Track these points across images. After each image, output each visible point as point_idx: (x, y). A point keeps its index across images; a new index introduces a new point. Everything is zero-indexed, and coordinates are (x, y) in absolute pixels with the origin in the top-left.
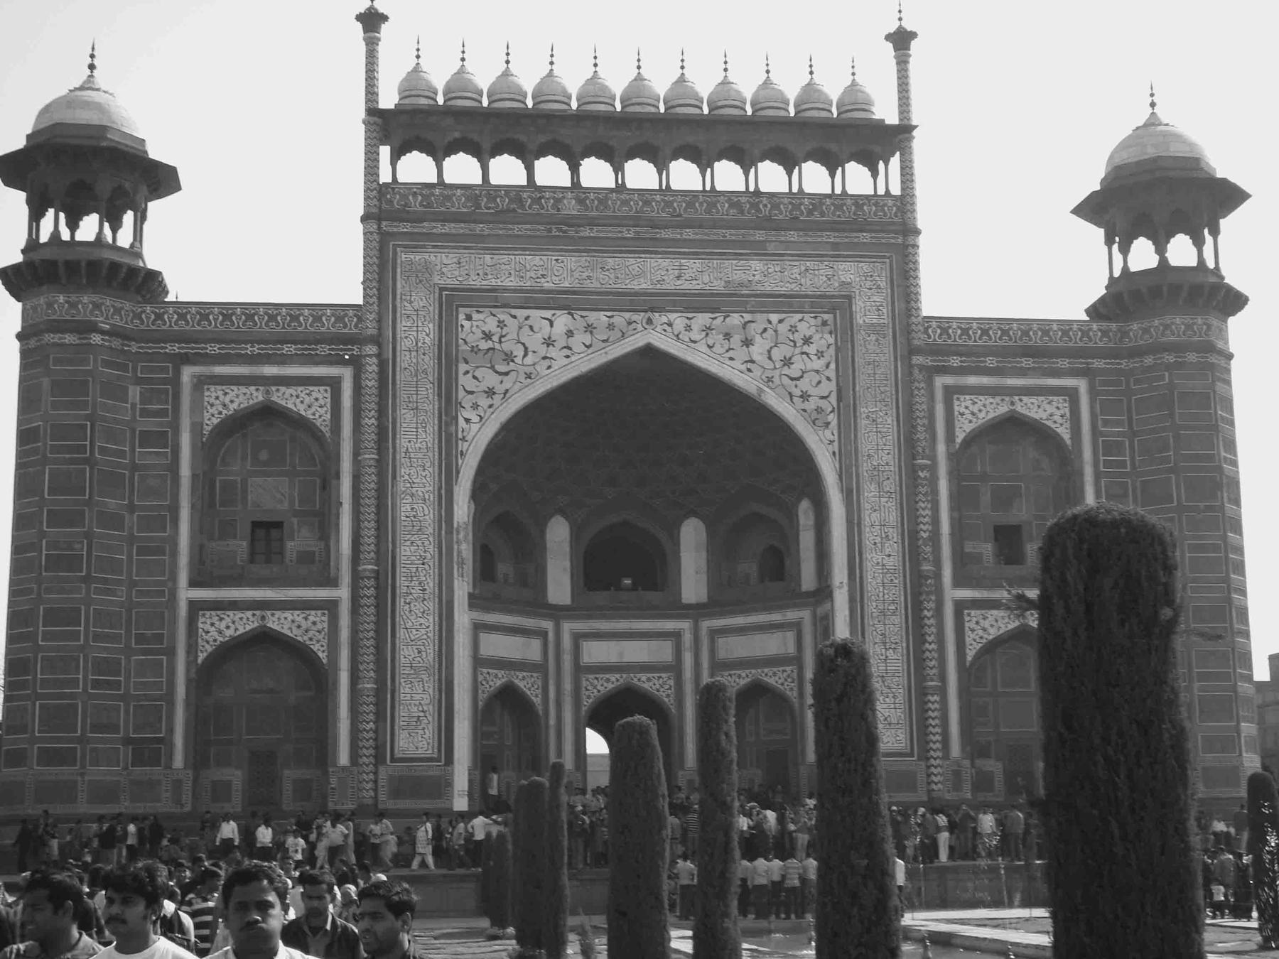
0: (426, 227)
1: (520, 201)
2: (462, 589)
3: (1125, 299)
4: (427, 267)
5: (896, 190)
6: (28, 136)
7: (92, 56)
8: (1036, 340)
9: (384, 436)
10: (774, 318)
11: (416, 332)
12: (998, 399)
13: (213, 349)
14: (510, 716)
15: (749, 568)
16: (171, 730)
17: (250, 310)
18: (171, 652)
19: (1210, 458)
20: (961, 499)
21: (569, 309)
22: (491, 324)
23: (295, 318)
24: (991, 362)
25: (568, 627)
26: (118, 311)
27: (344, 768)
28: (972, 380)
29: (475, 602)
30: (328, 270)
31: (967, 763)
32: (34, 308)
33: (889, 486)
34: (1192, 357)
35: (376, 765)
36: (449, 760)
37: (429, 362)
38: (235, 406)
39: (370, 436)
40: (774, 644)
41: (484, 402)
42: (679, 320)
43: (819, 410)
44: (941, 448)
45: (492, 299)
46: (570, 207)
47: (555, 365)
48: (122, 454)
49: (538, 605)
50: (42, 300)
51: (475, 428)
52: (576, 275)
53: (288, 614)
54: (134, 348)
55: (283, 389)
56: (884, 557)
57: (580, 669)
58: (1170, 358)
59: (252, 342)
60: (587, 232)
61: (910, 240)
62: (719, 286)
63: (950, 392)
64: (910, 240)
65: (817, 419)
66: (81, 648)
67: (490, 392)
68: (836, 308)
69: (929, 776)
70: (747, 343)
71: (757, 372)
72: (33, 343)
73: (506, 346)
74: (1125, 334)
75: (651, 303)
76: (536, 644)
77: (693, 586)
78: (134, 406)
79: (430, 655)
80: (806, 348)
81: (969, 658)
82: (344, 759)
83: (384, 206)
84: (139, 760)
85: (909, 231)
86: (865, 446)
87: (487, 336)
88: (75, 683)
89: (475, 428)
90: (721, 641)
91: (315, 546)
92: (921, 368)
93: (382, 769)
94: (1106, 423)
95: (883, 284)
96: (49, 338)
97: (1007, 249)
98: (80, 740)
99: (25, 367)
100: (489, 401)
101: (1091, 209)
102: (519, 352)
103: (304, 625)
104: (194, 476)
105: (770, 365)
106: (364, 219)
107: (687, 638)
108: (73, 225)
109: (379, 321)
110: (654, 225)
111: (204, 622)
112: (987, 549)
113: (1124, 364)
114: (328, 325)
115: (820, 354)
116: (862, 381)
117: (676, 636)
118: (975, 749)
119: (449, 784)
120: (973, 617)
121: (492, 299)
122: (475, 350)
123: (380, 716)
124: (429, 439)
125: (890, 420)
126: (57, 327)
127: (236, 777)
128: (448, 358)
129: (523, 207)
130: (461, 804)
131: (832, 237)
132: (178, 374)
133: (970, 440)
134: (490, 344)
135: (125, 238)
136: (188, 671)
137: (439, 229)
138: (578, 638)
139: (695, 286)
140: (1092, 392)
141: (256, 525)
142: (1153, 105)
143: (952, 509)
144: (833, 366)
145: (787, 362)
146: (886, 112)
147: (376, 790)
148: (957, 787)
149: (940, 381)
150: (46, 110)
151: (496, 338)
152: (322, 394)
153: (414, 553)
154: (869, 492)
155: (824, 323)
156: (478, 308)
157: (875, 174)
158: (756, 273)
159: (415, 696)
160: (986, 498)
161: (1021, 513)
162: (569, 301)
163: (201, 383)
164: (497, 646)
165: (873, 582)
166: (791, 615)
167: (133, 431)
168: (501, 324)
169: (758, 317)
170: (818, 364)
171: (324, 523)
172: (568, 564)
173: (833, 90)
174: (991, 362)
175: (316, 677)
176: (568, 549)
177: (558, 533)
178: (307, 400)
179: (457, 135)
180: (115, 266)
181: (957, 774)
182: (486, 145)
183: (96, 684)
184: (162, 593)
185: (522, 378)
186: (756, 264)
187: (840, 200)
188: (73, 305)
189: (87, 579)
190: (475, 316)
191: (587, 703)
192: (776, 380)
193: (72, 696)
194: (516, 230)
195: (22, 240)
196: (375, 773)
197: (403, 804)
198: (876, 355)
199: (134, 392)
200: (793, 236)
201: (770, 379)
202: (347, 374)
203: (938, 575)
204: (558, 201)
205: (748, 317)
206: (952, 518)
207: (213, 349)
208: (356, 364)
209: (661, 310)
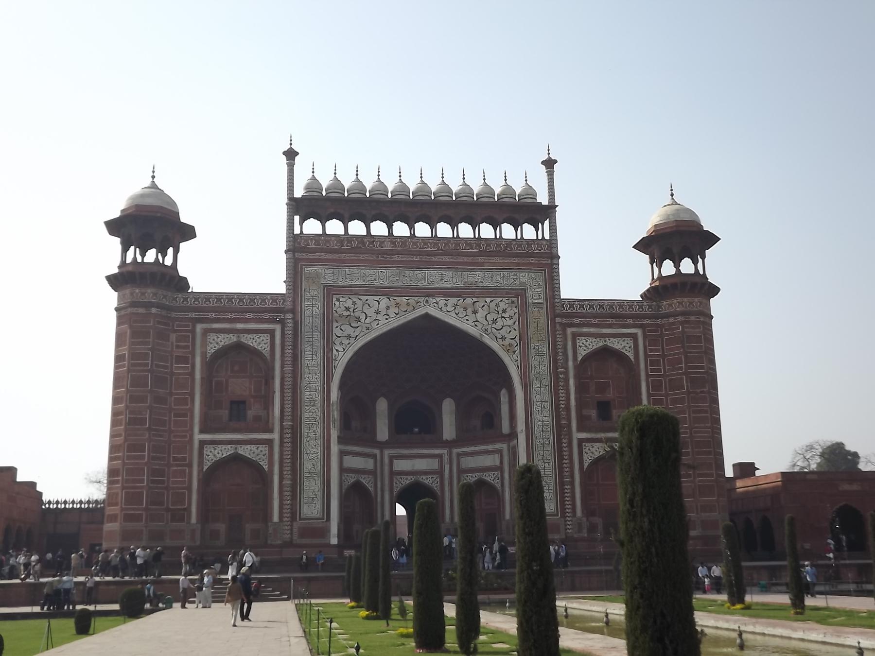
0: (317, 256)
1: (364, 244)
2: (334, 434)
3: (660, 290)
4: (318, 275)
5: (547, 237)
6: (122, 211)
7: (153, 172)
8: (617, 310)
9: (296, 358)
10: (488, 300)
11: (312, 308)
12: (598, 339)
13: (213, 315)
14: (358, 498)
16: (190, 504)
18: (190, 466)
19: (702, 367)
20: (581, 388)
21: (387, 295)
22: (349, 303)
23: (252, 300)
24: (594, 321)
25: (387, 452)
26: (165, 297)
27: (276, 523)
28: (585, 330)
29: (341, 440)
30: (268, 276)
31: (585, 519)
32: (124, 295)
33: (545, 382)
34: (693, 318)
35: (292, 522)
37: (318, 322)
38: (222, 343)
39: (289, 359)
41: (346, 341)
42: (442, 301)
43: (510, 345)
44: (571, 363)
46: (388, 246)
47: (381, 323)
48: (166, 367)
50: (127, 291)
51: (341, 354)
52: (391, 279)
53: (248, 446)
54: (173, 315)
55: (246, 335)
56: (543, 417)
57: (393, 473)
58: (681, 318)
59: (231, 312)
60: (396, 258)
61: (555, 261)
62: (460, 284)
63: (575, 336)
64: (555, 261)
65: (509, 350)
66: (146, 464)
67: (349, 337)
68: (519, 294)
69: (566, 525)
70: (475, 312)
71: (480, 326)
72: (123, 312)
73: (356, 314)
74: (660, 307)
75: (428, 293)
76: (371, 461)
77: (449, 431)
78: (172, 343)
80: (503, 315)
81: (586, 465)
82: (276, 519)
83: (297, 245)
84: (173, 520)
85: (554, 257)
86: (533, 362)
87: (347, 309)
88: (142, 481)
89: (341, 354)
90: (463, 459)
92: (561, 324)
93: (295, 524)
94: (651, 351)
95: (541, 283)
96: (130, 310)
97: (603, 267)
98: (146, 509)
99: (119, 324)
100: (348, 341)
101: (643, 246)
102: (363, 317)
103: (257, 452)
104: (202, 378)
105: (485, 323)
106: (286, 252)
107: (446, 458)
108: (143, 255)
109: (294, 302)
110: (429, 254)
111: (208, 450)
112: (593, 413)
113: (659, 321)
114: (269, 304)
115: (511, 317)
116: (532, 330)
117: (440, 457)
118: (589, 511)
119: (329, 531)
122: (341, 316)
123: (294, 496)
124: (319, 360)
125: (545, 350)
126: (133, 304)
127: (222, 527)
128: (328, 319)
129: (364, 246)
130: (334, 541)
131: (517, 260)
132: (194, 327)
133: (586, 358)
134: (348, 313)
135: (168, 261)
136: (198, 475)
137: (324, 256)
138: (392, 458)
139: (448, 285)
140: (645, 336)
141: (232, 403)
142: (672, 195)
143: (576, 392)
144: (517, 323)
146: (543, 198)
147: (291, 534)
148: (580, 530)
149: (569, 331)
151: (351, 310)
152: (266, 338)
153: (311, 415)
154: (535, 385)
155: (513, 302)
156: (343, 296)
157: (537, 230)
158: (477, 277)
159: (311, 487)
161: (610, 394)
162: (387, 292)
163: (206, 332)
165: (537, 430)
166: (497, 446)
167: (172, 356)
168: (354, 303)
169: (481, 299)
170: (510, 322)
172: (387, 421)
174: (594, 321)
175: (262, 477)
176: (386, 412)
177: (382, 406)
178: (258, 340)
179: (332, 210)
180: (163, 275)
181: (580, 525)
182: (347, 215)
183: (153, 482)
184: (185, 436)
185: (364, 330)
187: (520, 242)
188: (143, 294)
189: (149, 429)
190: (341, 299)
191: (396, 491)
192: (489, 330)
193: (142, 487)
194: (361, 257)
195: (118, 261)
196: (292, 526)
197: (305, 541)
198: (539, 317)
199: (173, 337)
200: (498, 260)
201: (486, 330)
202: (278, 328)
203: (569, 425)
204: (382, 243)
205: (475, 299)
206: (576, 399)
207: (213, 315)
208: (282, 322)
209: (433, 296)
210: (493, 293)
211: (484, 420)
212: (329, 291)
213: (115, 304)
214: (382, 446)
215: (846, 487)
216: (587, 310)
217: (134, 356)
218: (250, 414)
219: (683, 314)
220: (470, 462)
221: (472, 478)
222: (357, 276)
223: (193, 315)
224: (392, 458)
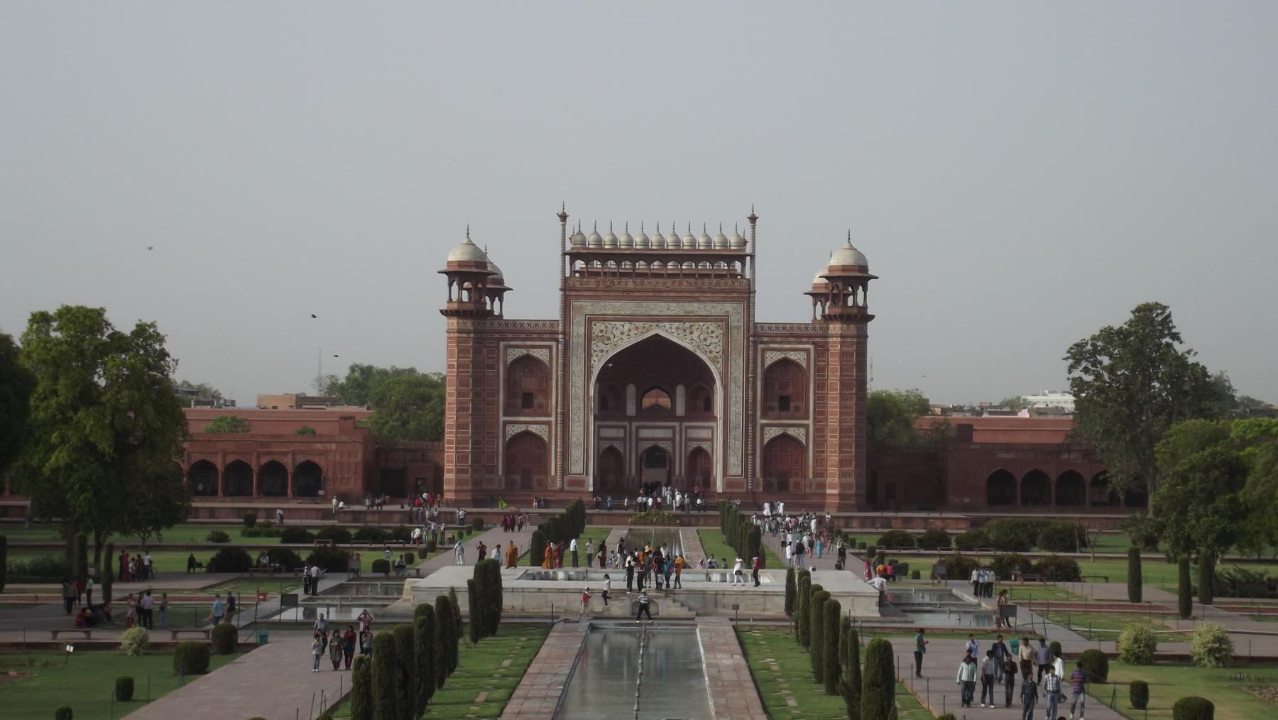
4: (581, 307)
8: (796, 331)
11: (578, 330)
13: (510, 336)
15: (701, 404)
17: (521, 323)
18: (497, 438)
21: (630, 321)
22: (603, 327)
25: (634, 424)
40: (705, 434)
42: (667, 325)
44: (759, 370)
45: (603, 318)
56: (737, 409)
57: (638, 439)
65: (714, 361)
68: (724, 320)
75: (658, 320)
82: (553, 473)
91: (544, 402)
107: (678, 429)
112: (776, 404)
114: (548, 327)
117: (673, 428)
121: (603, 318)
127: (518, 478)
128: (589, 338)
130: (591, 489)
138: (638, 428)
139: (673, 313)
140: (815, 350)
145: (705, 340)
149: (761, 346)
153: (577, 406)
154: (733, 386)
156: (598, 320)
158: (695, 308)
159: (576, 453)
161: (789, 391)
163: (506, 347)
165: (732, 417)
166: (711, 424)
177: (631, 390)
198: (738, 338)
199: (485, 350)
203: (754, 415)
207: (510, 336)
208: (557, 340)
210: (705, 319)
211: (701, 405)
212: (590, 321)
213: (445, 328)
214: (630, 419)
215: (1003, 455)
216: (774, 332)
217: (459, 366)
218: (536, 402)
219: (842, 336)
220: (694, 434)
221: (694, 445)
222: (610, 307)
223: (497, 336)
224: (638, 428)
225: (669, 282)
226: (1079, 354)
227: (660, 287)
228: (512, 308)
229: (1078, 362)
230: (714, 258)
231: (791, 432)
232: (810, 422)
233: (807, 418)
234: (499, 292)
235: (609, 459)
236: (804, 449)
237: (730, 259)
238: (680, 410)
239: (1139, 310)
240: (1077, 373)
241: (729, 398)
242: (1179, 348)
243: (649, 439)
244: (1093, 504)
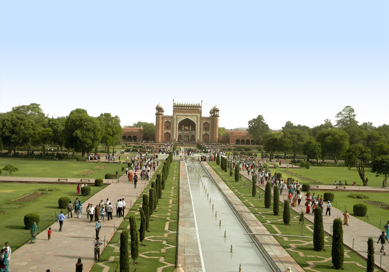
11: (175, 117)
15: (193, 129)
21: (183, 116)
25: (183, 131)
33: (199, 126)
36: (176, 139)
37: (176, 119)
40: (194, 133)
42: (189, 117)
45: (179, 116)
49: (182, 130)
56: (199, 129)
68: (197, 116)
75: (187, 116)
79: (176, 133)
85: (201, 112)
114: (171, 117)
120: (203, 133)
121: (179, 116)
127: (166, 139)
130: (177, 141)
149: (203, 120)
150: (157, 105)
153: (175, 128)
158: (193, 114)
159: (175, 136)
160: (205, 126)
164: (179, 133)
171: (171, 127)
173: (198, 104)
177: (183, 126)
186: (193, 114)
198: (199, 119)
210: (195, 116)
214: (183, 131)
215: (238, 137)
216: (205, 118)
218: (169, 128)
220: (192, 133)
221: (192, 135)
225: (189, 110)
226: (250, 122)
227: (188, 111)
228: (165, 114)
229: (250, 123)
230: (196, 107)
231: (207, 133)
232: (210, 131)
233: (209, 131)
234: (163, 111)
235: (180, 136)
236: (209, 136)
237: (198, 107)
238: (190, 129)
239: (259, 116)
240: (249, 125)
241: (198, 128)
242: (264, 122)
243: (186, 134)
244: (251, 144)
